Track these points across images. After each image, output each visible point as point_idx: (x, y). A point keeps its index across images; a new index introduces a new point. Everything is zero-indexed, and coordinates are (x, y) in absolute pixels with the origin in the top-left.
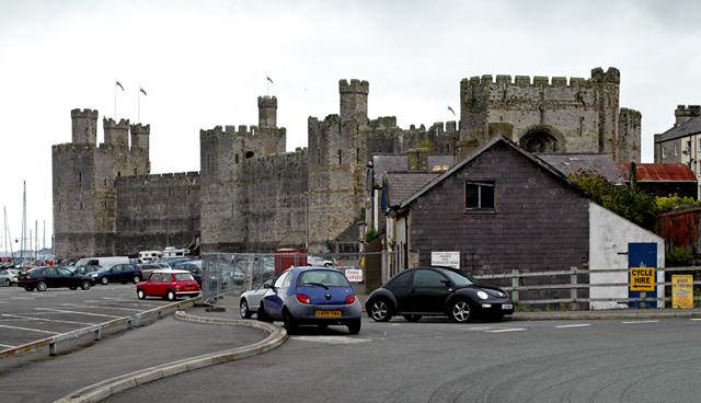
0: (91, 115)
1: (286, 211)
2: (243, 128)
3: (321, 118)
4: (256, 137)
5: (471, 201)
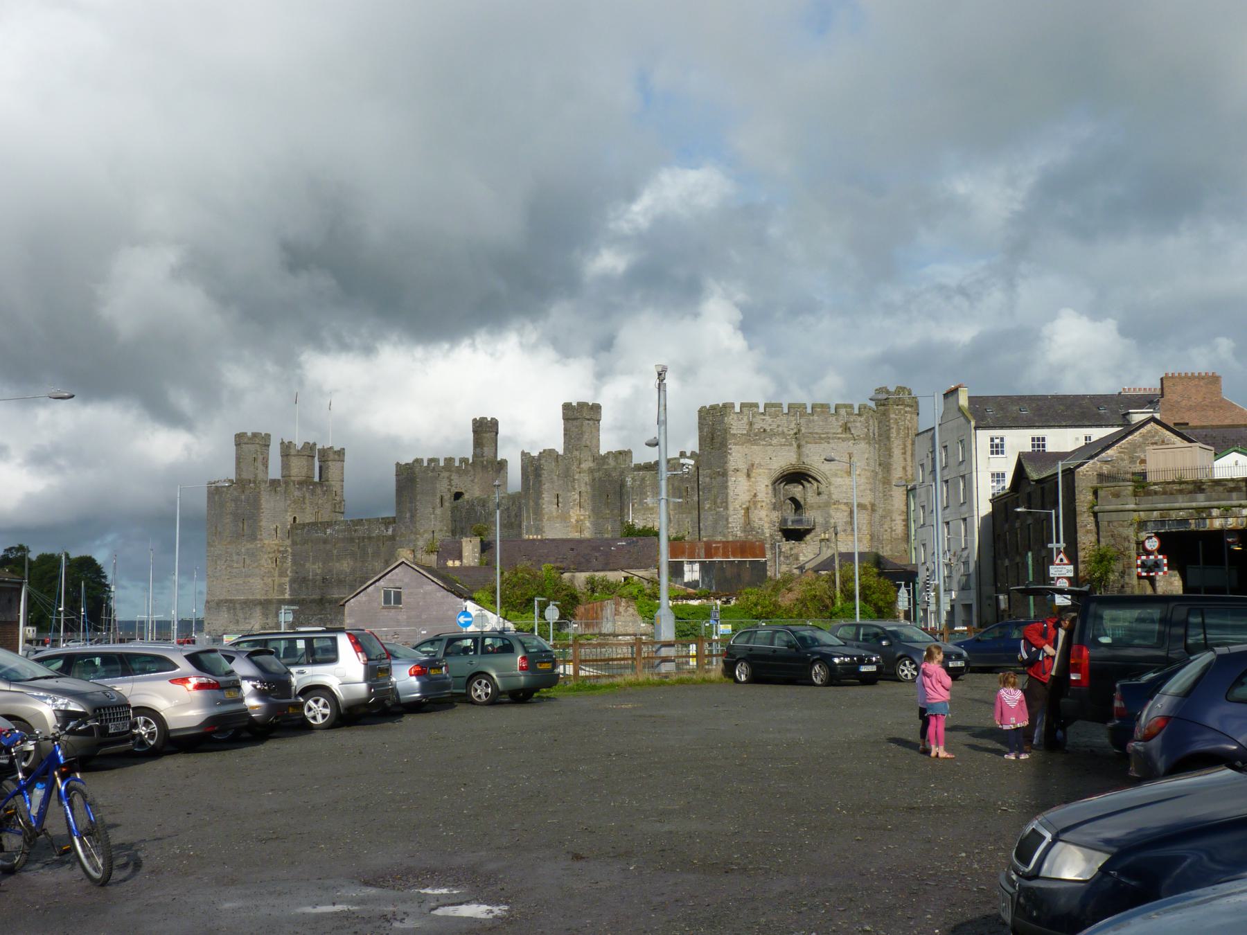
0: (263, 441)
2: (449, 461)
3: (535, 453)
4: (466, 472)
5: (387, 600)
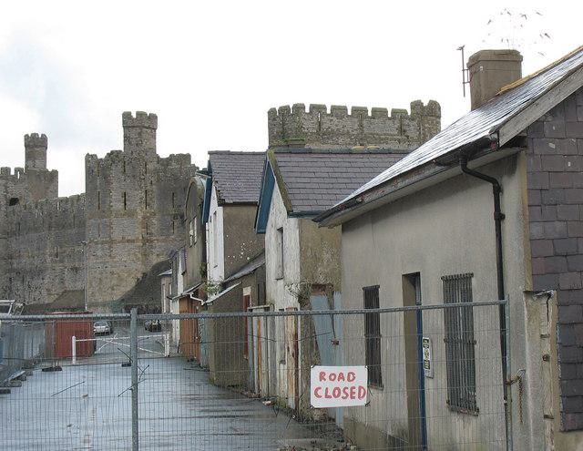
1: (58, 267)
